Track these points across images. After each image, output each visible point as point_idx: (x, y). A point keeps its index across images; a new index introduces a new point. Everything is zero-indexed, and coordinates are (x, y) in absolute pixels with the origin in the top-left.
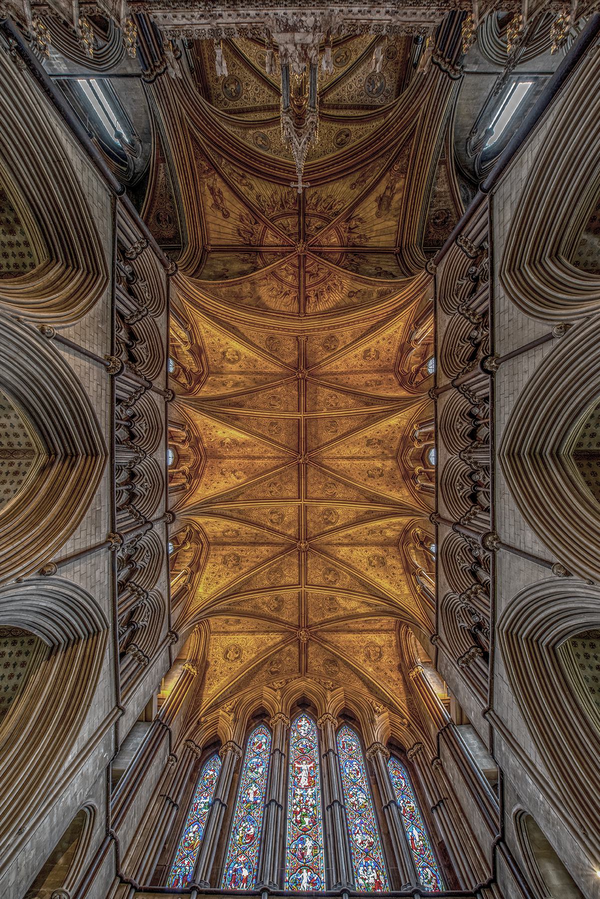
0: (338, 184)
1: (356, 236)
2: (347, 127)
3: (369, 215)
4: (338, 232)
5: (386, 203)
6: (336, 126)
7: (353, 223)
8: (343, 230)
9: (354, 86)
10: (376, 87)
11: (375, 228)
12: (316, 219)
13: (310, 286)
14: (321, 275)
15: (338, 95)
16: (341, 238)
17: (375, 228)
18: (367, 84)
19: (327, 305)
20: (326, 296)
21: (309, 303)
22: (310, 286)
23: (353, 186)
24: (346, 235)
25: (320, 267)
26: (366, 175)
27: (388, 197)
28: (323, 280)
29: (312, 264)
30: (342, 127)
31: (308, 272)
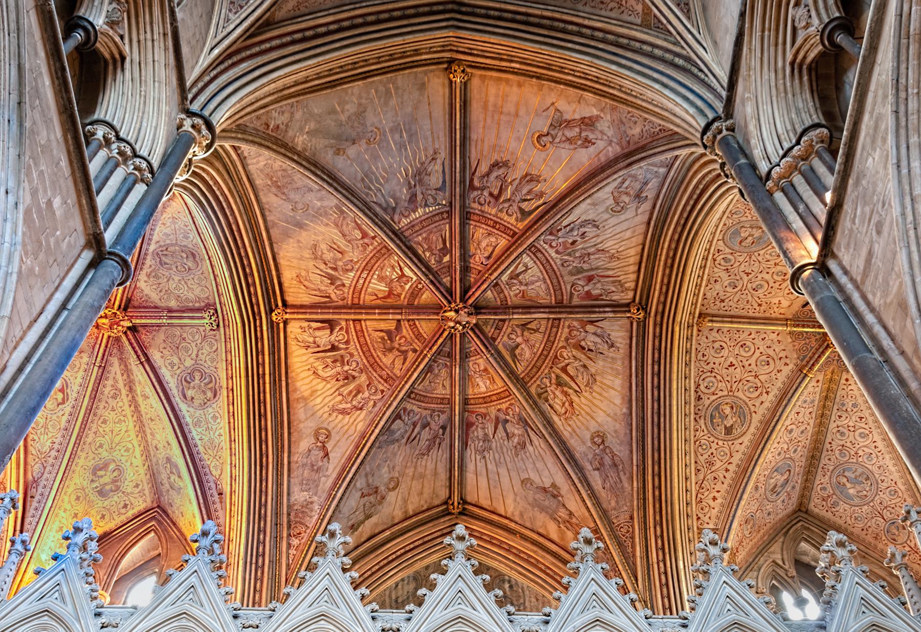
0: (618, 401)
1: (490, 431)
2: (752, 430)
3: (530, 466)
4: (500, 397)
5: (547, 503)
6: (767, 404)
7: (516, 430)
8: (504, 406)
9: (862, 442)
10: (848, 485)
11: (503, 471)
12: (539, 347)
13: (360, 333)
14: (387, 360)
15: (855, 405)
16: (486, 400)
17: (503, 471)
18: (860, 470)
19: (303, 375)
20: (329, 372)
21: (318, 329)
22: (360, 333)
23: (600, 438)
24: (493, 412)
25: (411, 355)
26: (612, 473)
27: (555, 512)
28: (375, 364)
29: (419, 336)
30: (756, 419)
31: (398, 327)
